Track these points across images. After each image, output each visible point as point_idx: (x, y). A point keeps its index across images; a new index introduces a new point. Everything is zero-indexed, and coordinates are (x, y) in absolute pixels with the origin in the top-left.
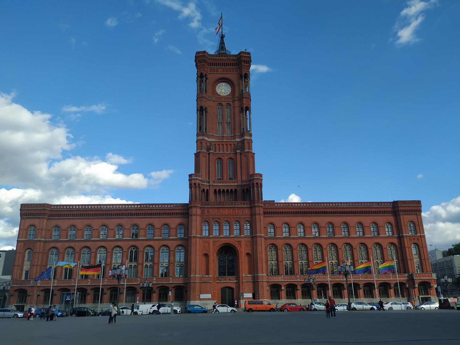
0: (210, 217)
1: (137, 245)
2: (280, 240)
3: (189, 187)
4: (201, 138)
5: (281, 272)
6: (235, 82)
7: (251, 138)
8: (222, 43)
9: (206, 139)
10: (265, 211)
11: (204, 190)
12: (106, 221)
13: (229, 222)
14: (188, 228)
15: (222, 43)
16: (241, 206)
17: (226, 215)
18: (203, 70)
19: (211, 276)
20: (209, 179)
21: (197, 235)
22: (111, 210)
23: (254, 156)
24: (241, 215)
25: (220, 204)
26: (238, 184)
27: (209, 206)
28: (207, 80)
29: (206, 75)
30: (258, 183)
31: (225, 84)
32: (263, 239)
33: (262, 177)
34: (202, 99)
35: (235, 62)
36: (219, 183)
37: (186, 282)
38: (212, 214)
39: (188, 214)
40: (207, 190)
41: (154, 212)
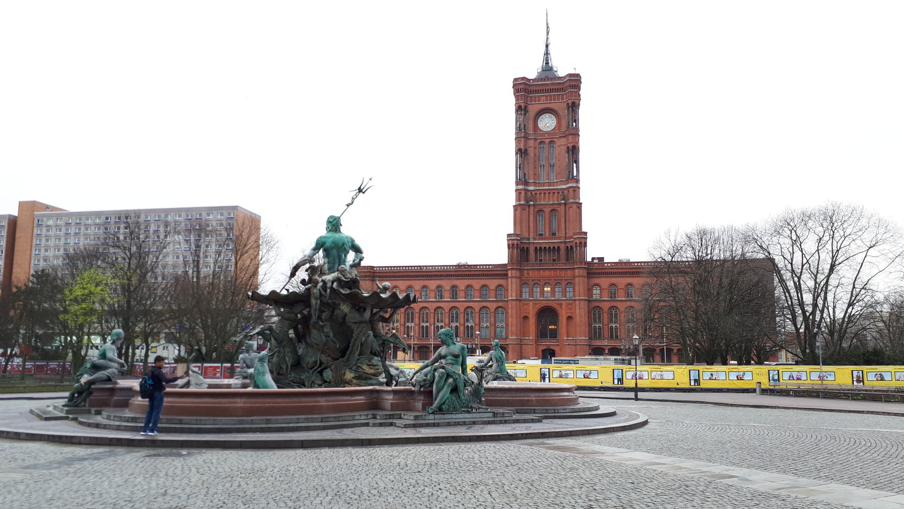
1: (458, 306)
2: (605, 303)
4: (520, 187)
5: (606, 336)
6: (560, 113)
8: (547, 53)
9: (526, 187)
10: (590, 271)
11: (523, 248)
12: (426, 283)
14: (507, 290)
15: (547, 53)
19: (531, 338)
20: (529, 236)
22: (431, 272)
23: (581, 207)
25: (540, 266)
29: (526, 107)
31: (549, 114)
32: (586, 302)
33: (586, 235)
36: (539, 240)
37: (508, 343)
39: (507, 275)
41: (473, 273)
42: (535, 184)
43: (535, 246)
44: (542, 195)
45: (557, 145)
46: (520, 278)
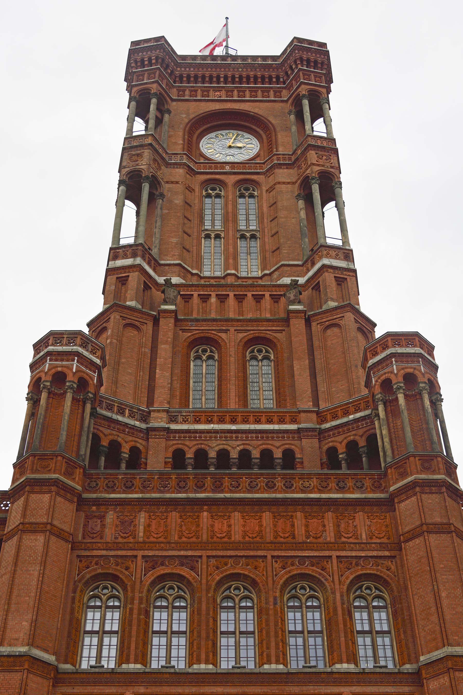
0: (135, 553)
3: (27, 399)
7: (351, 267)
13: (254, 583)
16: (324, 496)
17: (236, 546)
18: (153, 82)
20: (150, 401)
21: (38, 647)
24: (328, 546)
26: (302, 426)
27: (136, 493)
28: (166, 117)
30: (417, 372)
34: (139, 152)
35: (274, 74)
38: (152, 539)
40: (135, 451)
42: (184, 272)
43: (175, 444)
44: (213, 300)
45: (264, 189)
46: (74, 546)
